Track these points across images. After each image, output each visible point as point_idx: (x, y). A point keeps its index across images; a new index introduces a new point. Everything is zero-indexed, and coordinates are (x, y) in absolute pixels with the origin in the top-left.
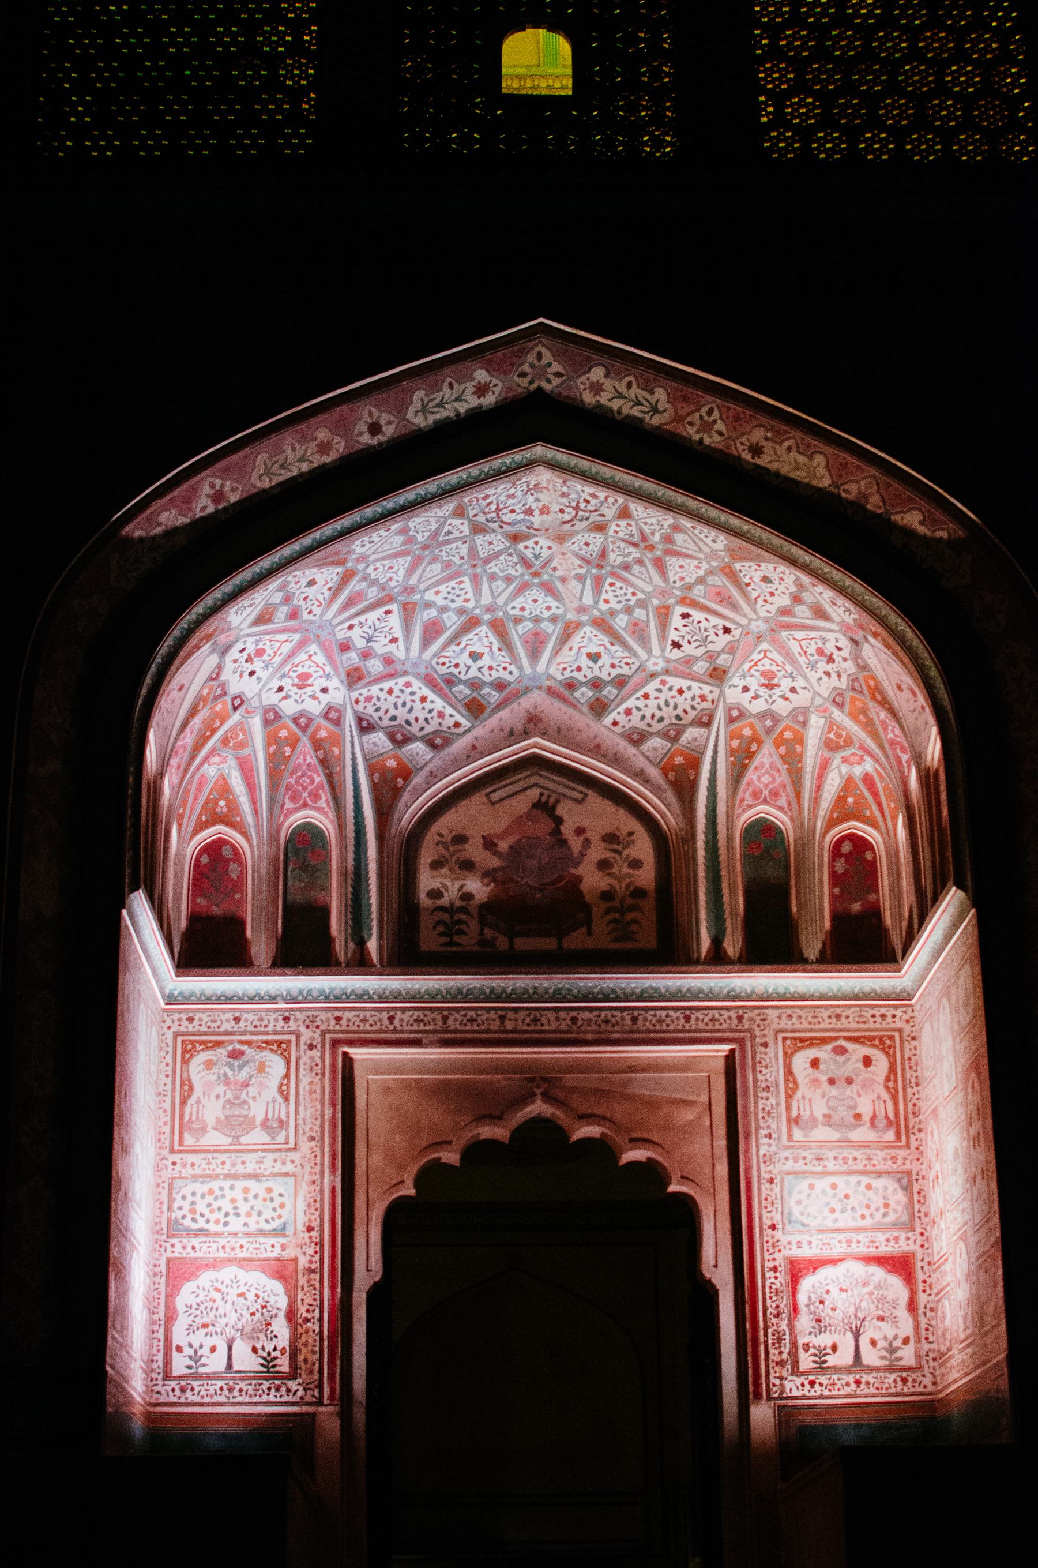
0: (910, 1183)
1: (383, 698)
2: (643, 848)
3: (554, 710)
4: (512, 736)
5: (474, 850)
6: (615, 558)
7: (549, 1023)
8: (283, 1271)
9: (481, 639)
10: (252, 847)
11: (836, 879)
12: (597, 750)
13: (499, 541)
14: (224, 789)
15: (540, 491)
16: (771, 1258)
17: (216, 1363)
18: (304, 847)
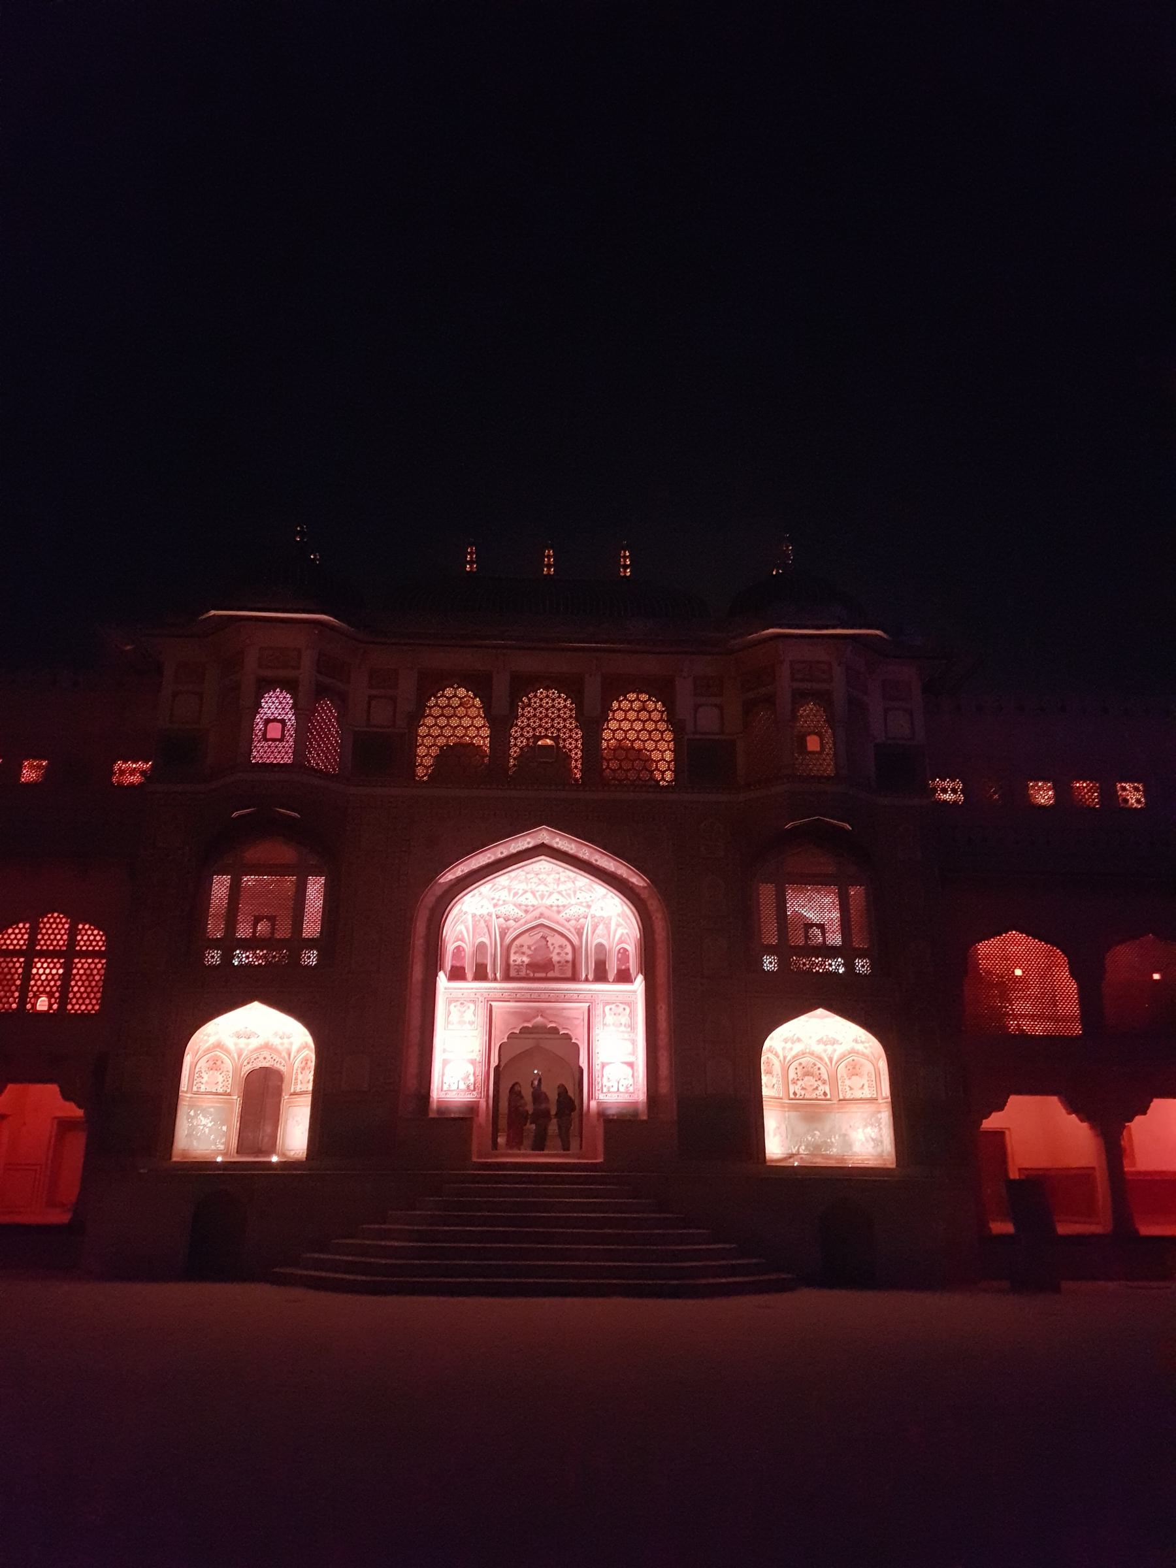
0: (633, 1042)
1: (502, 910)
2: (569, 949)
3: (547, 912)
4: (536, 918)
5: (525, 949)
6: (562, 879)
7: (543, 996)
8: (473, 1062)
9: (529, 895)
10: (468, 949)
11: (618, 959)
12: (558, 923)
13: (532, 875)
14: (461, 932)
15: (543, 866)
16: (597, 1061)
17: (454, 1087)
18: (481, 947)
